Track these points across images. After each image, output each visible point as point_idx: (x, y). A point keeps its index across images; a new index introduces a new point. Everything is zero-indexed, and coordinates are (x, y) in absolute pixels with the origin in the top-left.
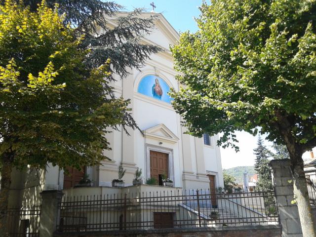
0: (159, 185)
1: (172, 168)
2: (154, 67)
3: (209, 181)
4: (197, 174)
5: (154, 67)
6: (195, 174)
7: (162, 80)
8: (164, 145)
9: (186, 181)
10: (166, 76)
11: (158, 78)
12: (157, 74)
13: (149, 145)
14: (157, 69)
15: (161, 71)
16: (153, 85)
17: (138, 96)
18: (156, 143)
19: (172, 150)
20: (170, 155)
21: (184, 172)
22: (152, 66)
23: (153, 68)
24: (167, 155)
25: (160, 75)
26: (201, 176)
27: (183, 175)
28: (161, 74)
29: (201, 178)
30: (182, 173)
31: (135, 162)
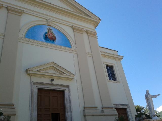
0: (84, 116)
1: (68, 105)
2: (46, 19)
3: (117, 114)
4: (102, 108)
5: (46, 19)
6: (99, 107)
7: (60, 32)
8: (56, 82)
9: (87, 117)
10: (61, 27)
11: (50, 27)
12: (49, 24)
13: (35, 83)
14: (48, 20)
15: (54, 23)
16: (44, 33)
17: (24, 40)
18: (47, 81)
19: (68, 87)
20: (66, 92)
21: (84, 108)
22: (45, 19)
23: (45, 20)
24: (63, 92)
25: (53, 25)
26: (106, 109)
27: (84, 110)
28: (54, 24)
29: (106, 112)
30: (82, 109)
31: (14, 102)
